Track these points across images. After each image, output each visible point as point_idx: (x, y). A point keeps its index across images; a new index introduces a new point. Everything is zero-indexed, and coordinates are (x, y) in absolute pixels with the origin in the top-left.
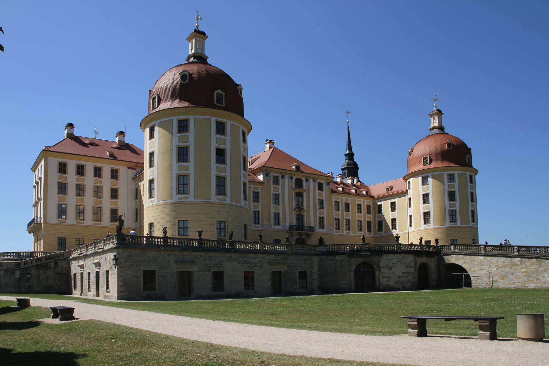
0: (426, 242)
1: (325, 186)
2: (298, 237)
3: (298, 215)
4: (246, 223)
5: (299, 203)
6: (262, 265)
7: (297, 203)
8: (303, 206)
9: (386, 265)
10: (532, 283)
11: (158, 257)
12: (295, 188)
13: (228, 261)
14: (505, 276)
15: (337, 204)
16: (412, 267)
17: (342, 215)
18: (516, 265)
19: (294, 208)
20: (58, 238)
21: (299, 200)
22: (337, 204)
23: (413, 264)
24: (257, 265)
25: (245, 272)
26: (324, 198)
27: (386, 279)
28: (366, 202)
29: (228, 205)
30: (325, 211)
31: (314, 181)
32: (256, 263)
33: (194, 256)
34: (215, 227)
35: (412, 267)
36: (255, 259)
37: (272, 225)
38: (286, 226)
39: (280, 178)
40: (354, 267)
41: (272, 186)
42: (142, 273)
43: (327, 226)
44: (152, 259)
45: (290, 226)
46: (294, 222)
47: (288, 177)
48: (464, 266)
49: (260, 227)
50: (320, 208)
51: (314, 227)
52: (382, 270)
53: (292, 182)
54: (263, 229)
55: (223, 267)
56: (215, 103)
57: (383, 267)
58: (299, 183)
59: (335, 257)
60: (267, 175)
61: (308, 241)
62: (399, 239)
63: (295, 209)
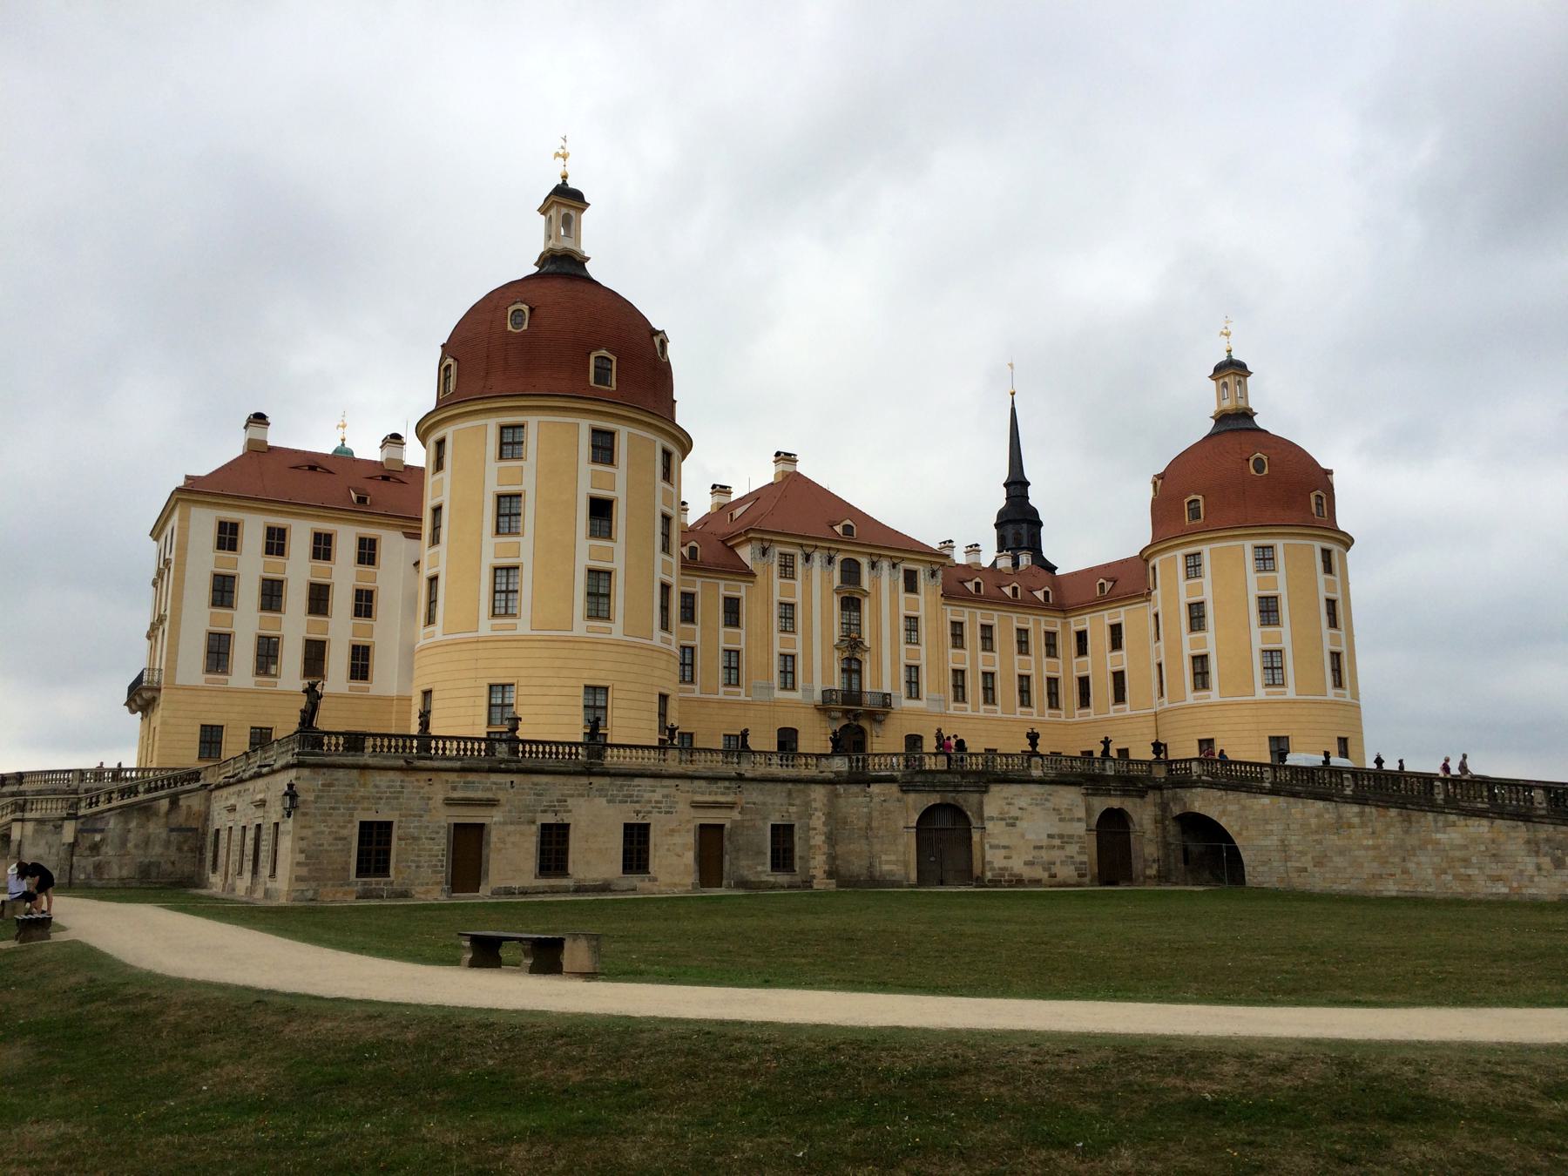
0: (1119, 751)
2: (845, 722)
3: (849, 659)
4: (665, 691)
5: (852, 627)
6: (671, 807)
7: (845, 626)
8: (860, 637)
9: (1001, 813)
10: (1391, 882)
11: (402, 787)
13: (583, 796)
14: (1326, 856)
15: (957, 627)
16: (1079, 820)
17: (974, 660)
18: (1350, 826)
19: (836, 641)
20: (202, 726)
22: (957, 627)
23: (1081, 813)
24: (660, 808)
25: (625, 824)
26: (921, 613)
27: (1003, 852)
28: (1043, 623)
29: (617, 644)
30: (923, 649)
31: (894, 566)
32: (657, 802)
33: (495, 783)
34: (581, 703)
35: (1079, 820)
36: (654, 791)
37: (774, 688)
39: (799, 561)
40: (917, 817)
41: (777, 582)
42: (357, 830)
43: (928, 691)
44: (386, 792)
46: (837, 683)
47: (821, 557)
48: (1223, 822)
49: (741, 694)
50: (909, 642)
51: (890, 695)
52: (989, 825)
53: (833, 571)
55: (570, 811)
56: (592, 384)
57: (992, 819)
58: (851, 572)
59: (869, 786)
60: (764, 552)
61: (874, 734)
62: (1038, 741)
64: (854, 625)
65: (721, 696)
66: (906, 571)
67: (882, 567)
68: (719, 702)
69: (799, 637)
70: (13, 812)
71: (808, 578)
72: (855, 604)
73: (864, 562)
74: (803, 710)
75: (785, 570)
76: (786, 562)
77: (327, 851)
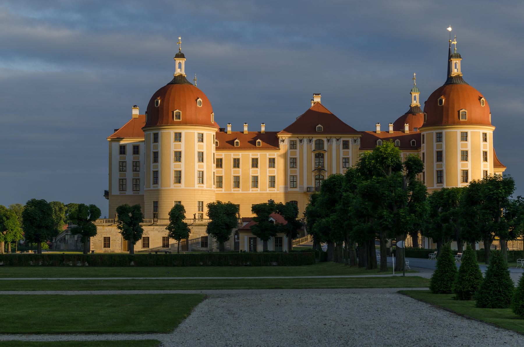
1: (352, 143)
7: (317, 164)
12: (314, 150)
19: (313, 169)
21: (319, 161)
26: (350, 156)
31: (338, 140)
37: (288, 187)
38: (304, 187)
45: (308, 188)
47: (307, 140)
54: (279, 192)
58: (319, 144)
63: (314, 171)
64: (321, 163)
65: (268, 191)
66: (343, 141)
67: (333, 141)
68: (267, 193)
69: (298, 170)
70: (66, 233)
71: (302, 148)
72: (322, 155)
73: (325, 140)
74: (299, 194)
75: (293, 146)
76: (293, 143)
77: (97, 243)
